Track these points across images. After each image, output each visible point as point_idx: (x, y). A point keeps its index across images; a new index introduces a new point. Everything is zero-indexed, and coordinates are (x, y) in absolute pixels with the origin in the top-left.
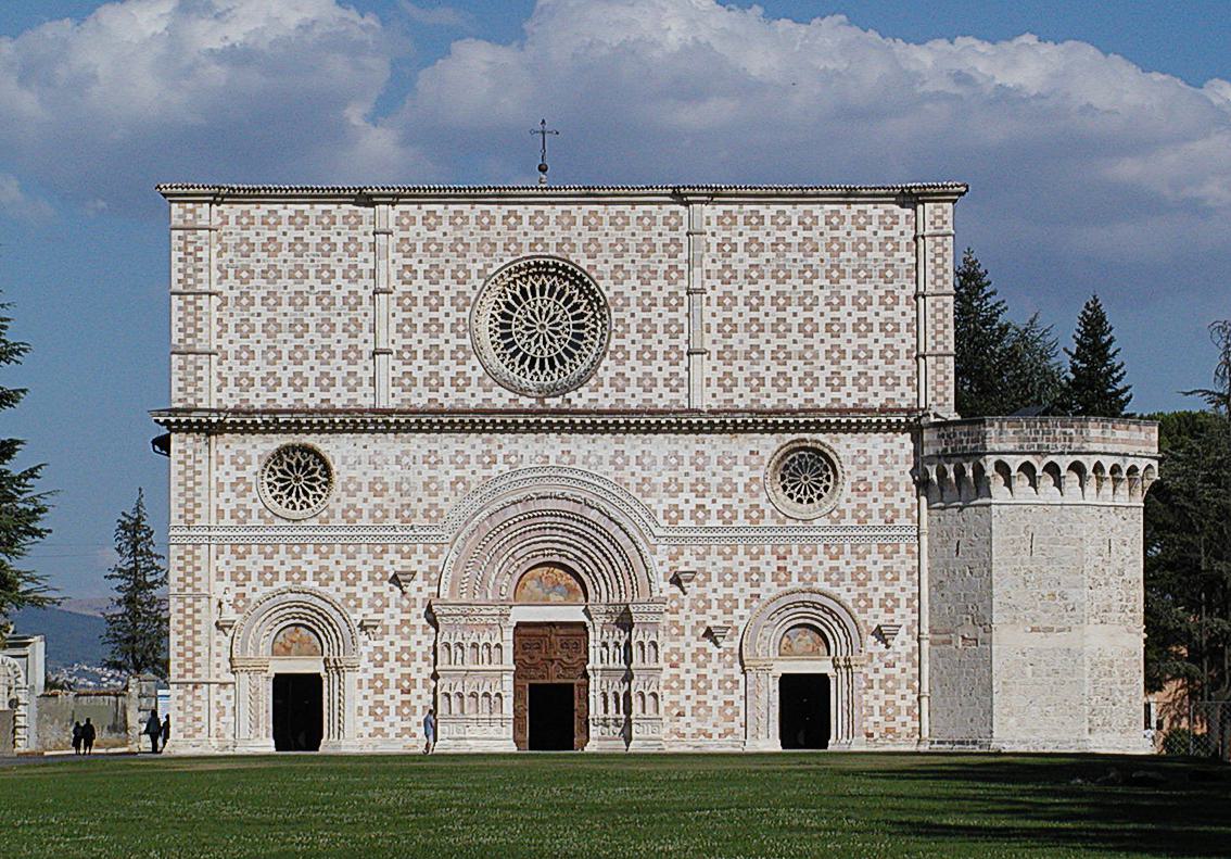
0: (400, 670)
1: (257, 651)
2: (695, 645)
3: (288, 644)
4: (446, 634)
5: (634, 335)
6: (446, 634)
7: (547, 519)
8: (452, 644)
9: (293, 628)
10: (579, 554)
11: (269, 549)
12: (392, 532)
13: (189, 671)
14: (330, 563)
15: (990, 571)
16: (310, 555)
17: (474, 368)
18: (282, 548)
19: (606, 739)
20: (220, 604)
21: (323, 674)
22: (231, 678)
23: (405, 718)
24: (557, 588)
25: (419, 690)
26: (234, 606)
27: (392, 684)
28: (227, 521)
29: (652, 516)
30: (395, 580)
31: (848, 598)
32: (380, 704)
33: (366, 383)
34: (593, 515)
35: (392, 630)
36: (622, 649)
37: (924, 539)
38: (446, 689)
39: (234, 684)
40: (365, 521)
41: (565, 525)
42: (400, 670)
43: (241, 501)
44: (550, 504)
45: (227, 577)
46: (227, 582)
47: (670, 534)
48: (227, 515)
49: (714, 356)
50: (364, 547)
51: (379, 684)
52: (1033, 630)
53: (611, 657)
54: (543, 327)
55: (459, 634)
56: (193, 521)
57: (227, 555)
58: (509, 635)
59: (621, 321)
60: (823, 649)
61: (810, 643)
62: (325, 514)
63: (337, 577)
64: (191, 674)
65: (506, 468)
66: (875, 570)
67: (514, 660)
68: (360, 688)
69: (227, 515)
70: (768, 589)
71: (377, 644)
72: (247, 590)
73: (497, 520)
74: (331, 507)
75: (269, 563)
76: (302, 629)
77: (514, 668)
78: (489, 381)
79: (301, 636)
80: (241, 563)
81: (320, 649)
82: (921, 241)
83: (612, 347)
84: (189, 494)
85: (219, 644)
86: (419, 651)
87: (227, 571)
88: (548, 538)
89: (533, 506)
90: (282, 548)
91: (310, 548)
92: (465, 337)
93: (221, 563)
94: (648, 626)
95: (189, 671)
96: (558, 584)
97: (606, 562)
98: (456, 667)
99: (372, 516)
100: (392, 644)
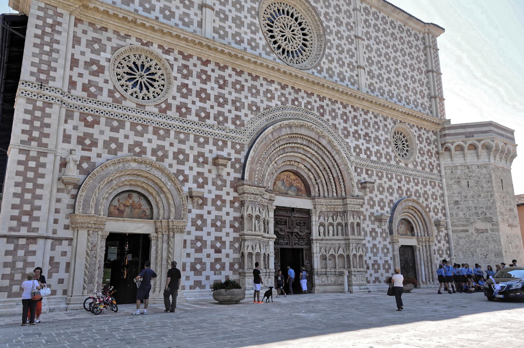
0: (215, 234)
1: (97, 211)
2: (371, 226)
3: (122, 208)
4: (250, 208)
5: (334, 50)
6: (250, 208)
7: (299, 141)
8: (254, 216)
9: (126, 195)
10: (309, 167)
11: (115, 124)
12: (211, 130)
13: (24, 224)
14: (166, 144)
15: (492, 196)
16: (150, 135)
17: (260, 39)
18: (128, 125)
19: (325, 285)
20: (64, 164)
21: (153, 235)
22: (68, 234)
23: (217, 272)
24: (293, 188)
25: (227, 250)
26: (79, 167)
27: (209, 244)
28: (78, 92)
29: (349, 148)
30: (216, 162)
31: (424, 205)
32: (199, 261)
33: (195, 24)
34: (324, 142)
35: (209, 202)
36: (335, 227)
37: (444, 180)
38: (250, 250)
39: (71, 240)
40: (193, 117)
41: (308, 147)
42: (215, 234)
43: (94, 79)
44: (303, 131)
45: (74, 140)
46: (73, 144)
47: (357, 161)
48: (79, 86)
49: (367, 73)
50: (192, 137)
51: (199, 244)
52: (509, 226)
53: (327, 231)
54: (288, 33)
55: (257, 209)
56: (47, 81)
57: (75, 121)
58: (272, 214)
59: (329, 41)
60: (409, 233)
61: (404, 229)
62: (163, 106)
63: (171, 155)
64: (26, 228)
65: (279, 103)
66: (430, 193)
67: (276, 233)
68: (185, 247)
69: (79, 86)
70: (395, 197)
71: (199, 212)
72: (92, 154)
73: (276, 135)
74: (169, 102)
75: (114, 135)
76: (135, 195)
77: (275, 236)
78: (268, 50)
79: (133, 201)
80: (90, 130)
81: (148, 212)
82: (428, 49)
83: (326, 53)
84: (45, 58)
85: (58, 201)
86: (228, 219)
87: (74, 135)
88: (296, 154)
89: (295, 130)
90: (128, 125)
91: (151, 129)
92: (255, 18)
93: (69, 127)
94: (355, 213)
95: (24, 224)
96: (293, 185)
97: (324, 173)
98: (257, 233)
99: (197, 115)
100: (209, 213)
